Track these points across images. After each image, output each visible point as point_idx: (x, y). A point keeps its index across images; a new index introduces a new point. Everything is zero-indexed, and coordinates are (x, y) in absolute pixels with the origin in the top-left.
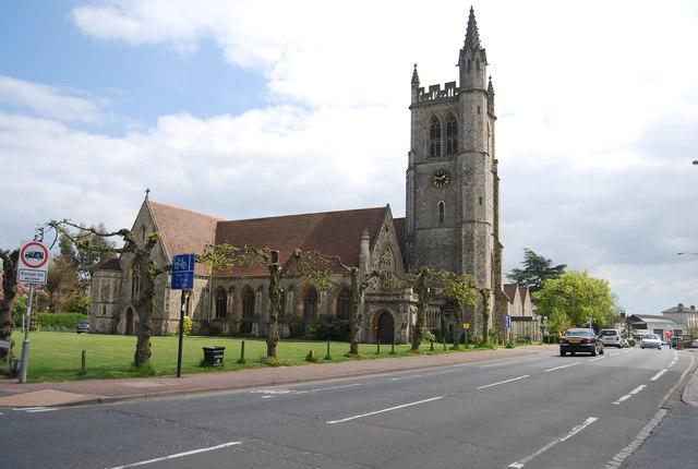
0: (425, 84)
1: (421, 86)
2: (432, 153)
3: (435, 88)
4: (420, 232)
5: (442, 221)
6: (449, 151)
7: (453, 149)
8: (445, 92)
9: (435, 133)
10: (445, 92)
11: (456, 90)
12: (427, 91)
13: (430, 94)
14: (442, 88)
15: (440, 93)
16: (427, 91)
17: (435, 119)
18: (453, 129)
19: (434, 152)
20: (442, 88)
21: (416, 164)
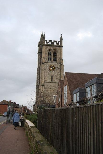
0: (48, 38)
1: (45, 39)
2: (48, 60)
4: (45, 83)
5: (52, 80)
6: (54, 60)
7: (55, 60)
8: (53, 43)
9: (49, 54)
10: (53, 43)
11: (57, 43)
12: (48, 41)
13: (48, 43)
14: (53, 42)
15: (52, 43)
16: (48, 41)
17: (50, 50)
18: (55, 55)
19: (49, 59)
20: (53, 42)
21: (44, 62)
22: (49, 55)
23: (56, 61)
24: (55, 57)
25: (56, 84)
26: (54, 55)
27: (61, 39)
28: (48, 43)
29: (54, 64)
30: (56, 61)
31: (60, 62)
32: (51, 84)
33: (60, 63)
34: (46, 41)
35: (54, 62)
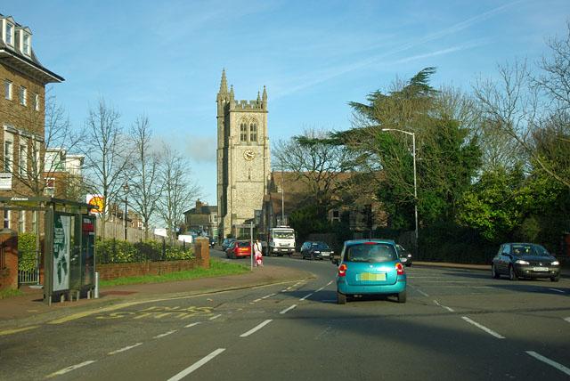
3: (245, 102)
6: (251, 139)
7: (254, 138)
9: (243, 128)
18: (253, 128)
19: (244, 138)
22: (242, 130)
23: (255, 140)
24: (253, 132)
25: (257, 185)
26: (251, 130)
27: (265, 96)
28: (241, 106)
29: (253, 146)
30: (255, 140)
31: (263, 143)
32: (249, 185)
33: (264, 145)
34: (236, 102)
35: (252, 143)
